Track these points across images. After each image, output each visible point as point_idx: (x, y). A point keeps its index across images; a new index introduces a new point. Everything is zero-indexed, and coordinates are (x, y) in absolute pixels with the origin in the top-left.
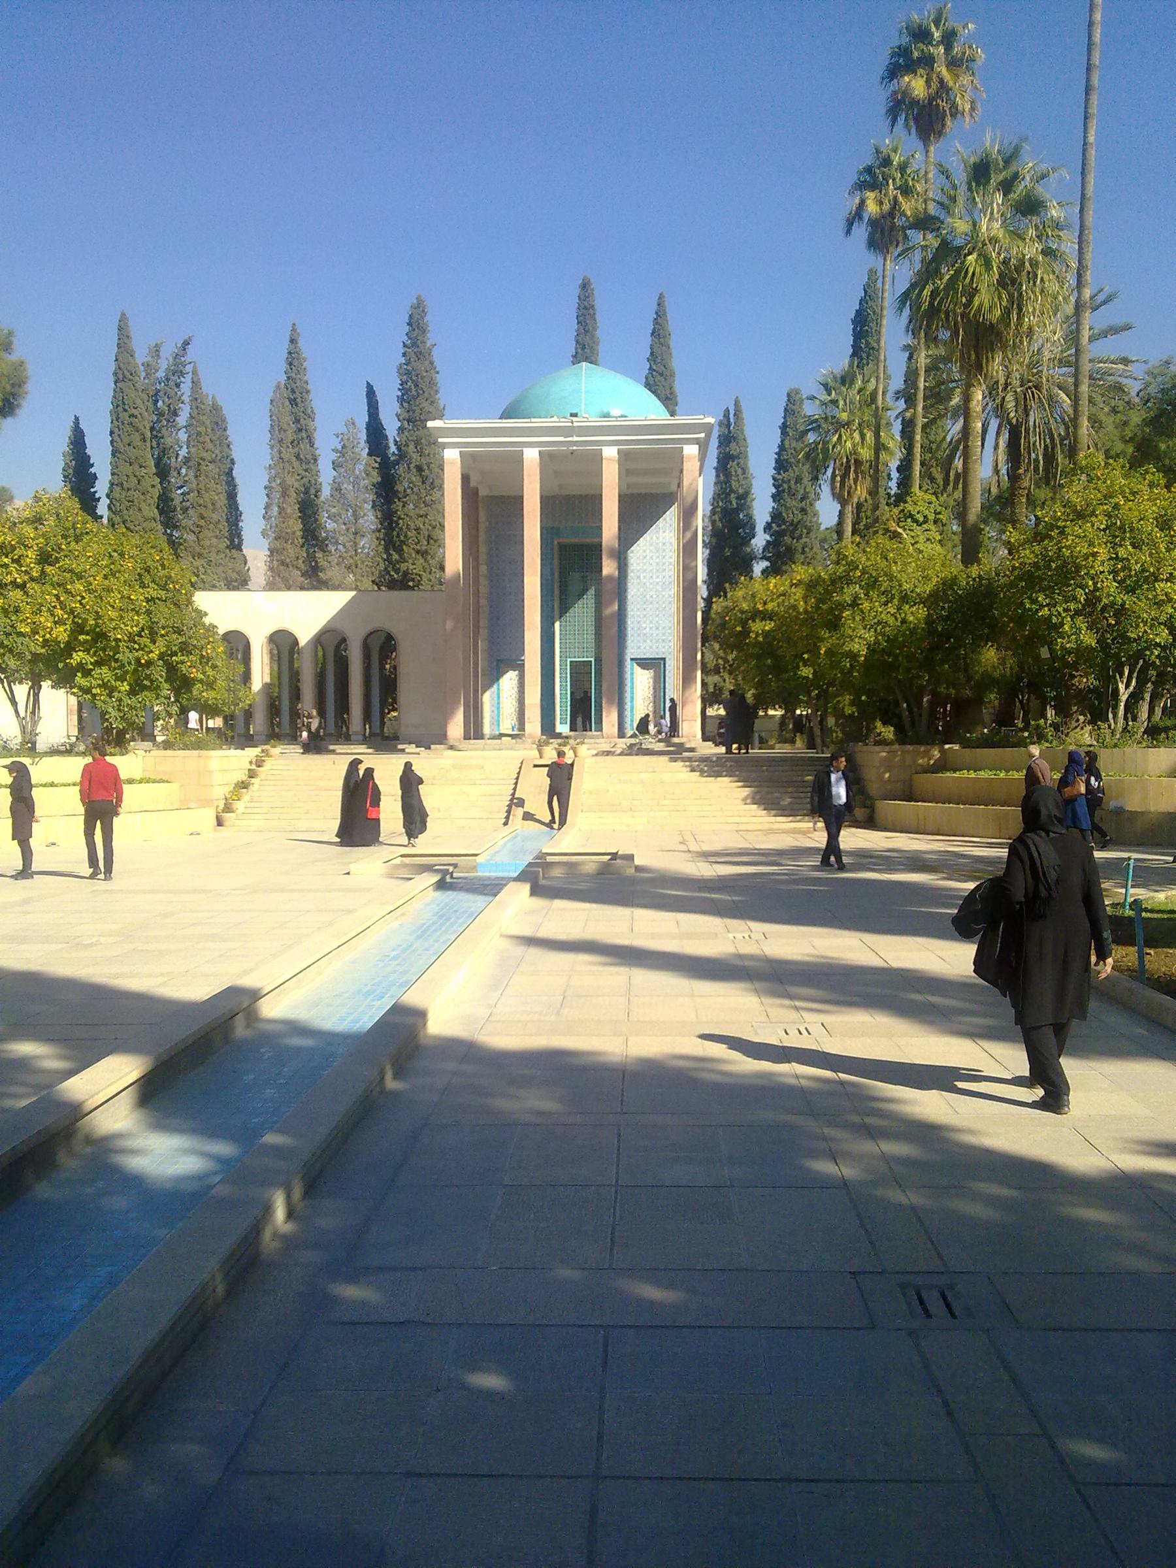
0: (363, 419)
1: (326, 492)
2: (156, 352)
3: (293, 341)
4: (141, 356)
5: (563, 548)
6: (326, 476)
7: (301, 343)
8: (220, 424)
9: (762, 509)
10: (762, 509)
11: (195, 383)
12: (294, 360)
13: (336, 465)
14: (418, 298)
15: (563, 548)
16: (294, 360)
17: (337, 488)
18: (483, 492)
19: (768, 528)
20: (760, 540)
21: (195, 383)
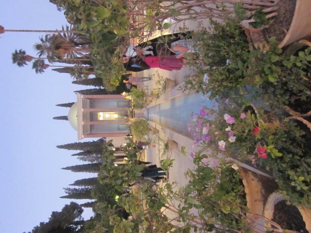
0: (77, 156)
1: (90, 163)
2: (66, 193)
3: (63, 169)
4: (68, 195)
6: (87, 163)
7: (64, 167)
8: (78, 181)
9: (92, 87)
10: (92, 87)
11: (72, 185)
12: (67, 168)
13: (85, 161)
14: (57, 147)
16: (67, 168)
17: (89, 161)
18: (89, 132)
19: (95, 87)
20: (97, 88)
21: (72, 185)
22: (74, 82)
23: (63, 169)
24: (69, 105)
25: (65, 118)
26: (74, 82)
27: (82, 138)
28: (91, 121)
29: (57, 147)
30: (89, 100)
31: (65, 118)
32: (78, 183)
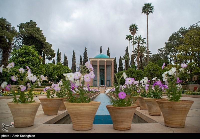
3: (74, 51)
4: (60, 52)
5: (100, 69)
7: (75, 52)
8: (67, 58)
9: (118, 67)
10: (118, 67)
12: (74, 53)
14: (86, 48)
15: (100, 69)
18: (93, 64)
20: (118, 70)
22: (120, 57)
23: (74, 51)
24: (108, 54)
25: (101, 52)
26: (120, 57)
27: (90, 60)
28: (99, 65)
29: (86, 48)
30: (111, 64)
31: (101, 52)
32: (66, 59)
